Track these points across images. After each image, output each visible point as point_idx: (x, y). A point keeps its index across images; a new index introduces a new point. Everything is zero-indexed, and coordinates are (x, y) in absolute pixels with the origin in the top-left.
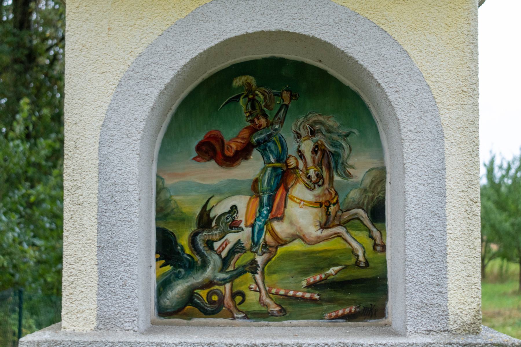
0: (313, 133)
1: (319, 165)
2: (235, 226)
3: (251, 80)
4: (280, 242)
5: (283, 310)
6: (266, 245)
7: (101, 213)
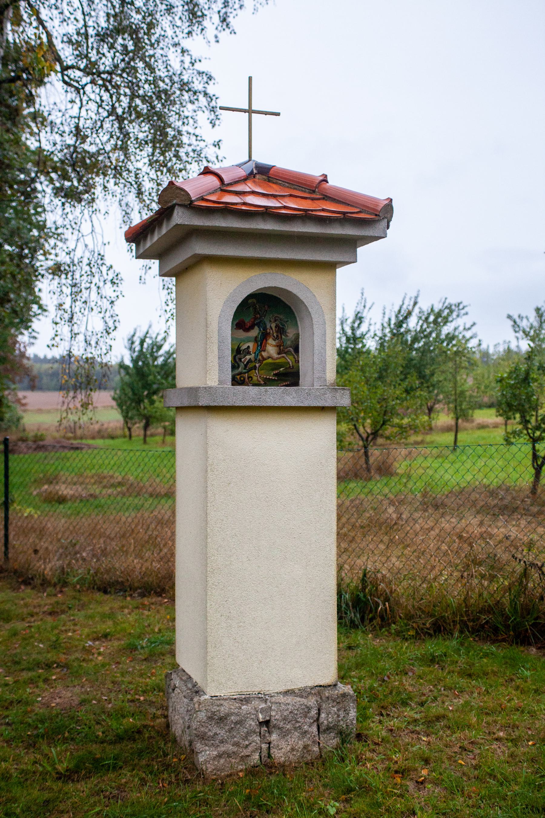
0: (275, 321)
1: (277, 332)
2: (249, 353)
3: (254, 301)
4: (264, 359)
6: (259, 360)
7: (219, 346)
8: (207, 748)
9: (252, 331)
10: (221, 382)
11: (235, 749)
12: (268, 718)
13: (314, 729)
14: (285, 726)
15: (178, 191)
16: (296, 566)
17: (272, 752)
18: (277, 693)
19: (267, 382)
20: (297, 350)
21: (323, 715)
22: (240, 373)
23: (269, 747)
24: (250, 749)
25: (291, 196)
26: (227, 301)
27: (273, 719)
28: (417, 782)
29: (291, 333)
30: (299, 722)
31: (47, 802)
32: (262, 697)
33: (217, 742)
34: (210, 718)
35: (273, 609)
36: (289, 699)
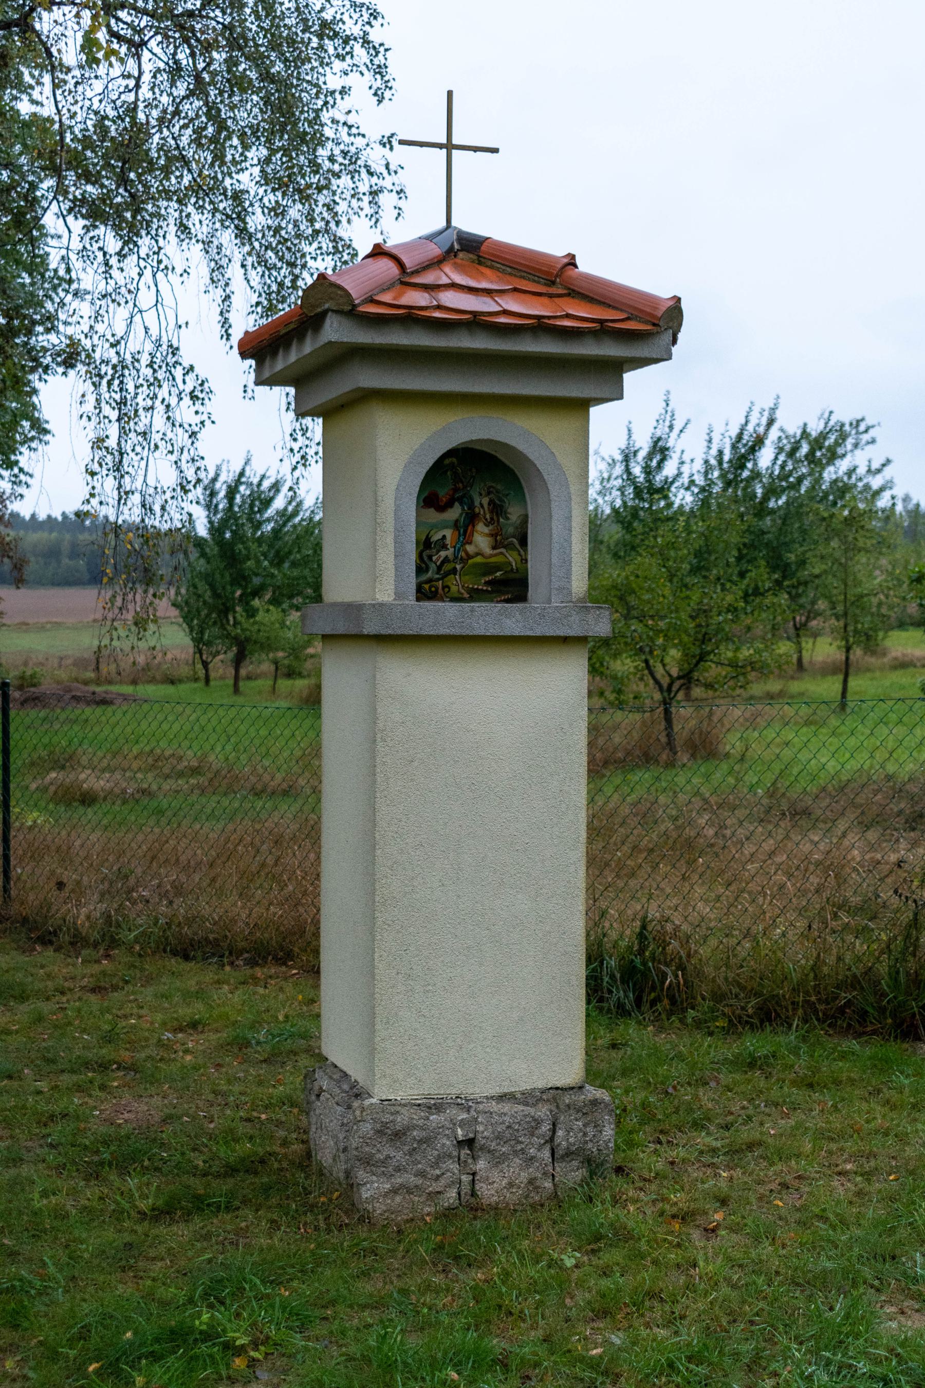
1: (491, 512)
2: (445, 547)
3: (454, 460)
4: (469, 557)
5: (471, 597)
6: (462, 558)
7: (396, 537)
8: (374, 1178)
9: (450, 510)
10: (398, 595)
11: (420, 1182)
12: (471, 1135)
13: (546, 1154)
14: (499, 1148)
15: (333, 289)
16: (519, 896)
17: (477, 1187)
18: (487, 1098)
19: (475, 595)
20: (523, 541)
21: (560, 1133)
22: (430, 581)
23: (473, 1180)
24: (442, 1182)
25: (515, 290)
26: (410, 463)
27: (479, 1136)
28: (706, 1230)
29: (514, 513)
30: (521, 1143)
31: (129, 1246)
32: (463, 1103)
33: (390, 1169)
34: (380, 1133)
35: (481, 964)
36: (506, 1107)
